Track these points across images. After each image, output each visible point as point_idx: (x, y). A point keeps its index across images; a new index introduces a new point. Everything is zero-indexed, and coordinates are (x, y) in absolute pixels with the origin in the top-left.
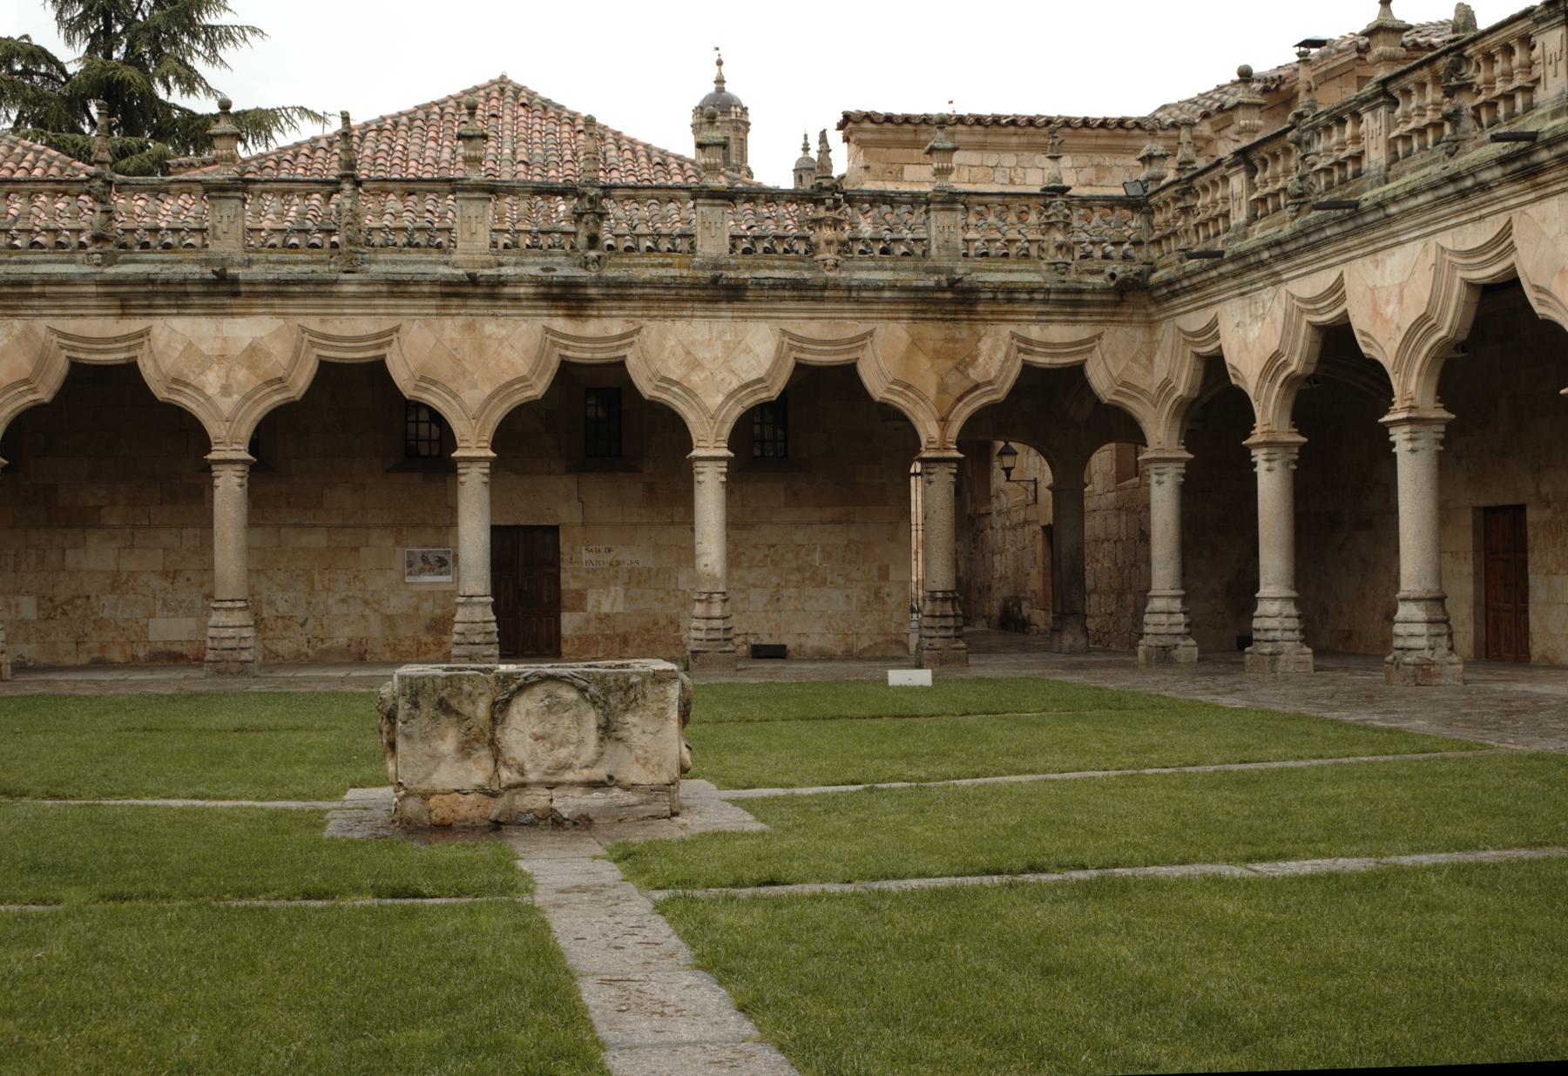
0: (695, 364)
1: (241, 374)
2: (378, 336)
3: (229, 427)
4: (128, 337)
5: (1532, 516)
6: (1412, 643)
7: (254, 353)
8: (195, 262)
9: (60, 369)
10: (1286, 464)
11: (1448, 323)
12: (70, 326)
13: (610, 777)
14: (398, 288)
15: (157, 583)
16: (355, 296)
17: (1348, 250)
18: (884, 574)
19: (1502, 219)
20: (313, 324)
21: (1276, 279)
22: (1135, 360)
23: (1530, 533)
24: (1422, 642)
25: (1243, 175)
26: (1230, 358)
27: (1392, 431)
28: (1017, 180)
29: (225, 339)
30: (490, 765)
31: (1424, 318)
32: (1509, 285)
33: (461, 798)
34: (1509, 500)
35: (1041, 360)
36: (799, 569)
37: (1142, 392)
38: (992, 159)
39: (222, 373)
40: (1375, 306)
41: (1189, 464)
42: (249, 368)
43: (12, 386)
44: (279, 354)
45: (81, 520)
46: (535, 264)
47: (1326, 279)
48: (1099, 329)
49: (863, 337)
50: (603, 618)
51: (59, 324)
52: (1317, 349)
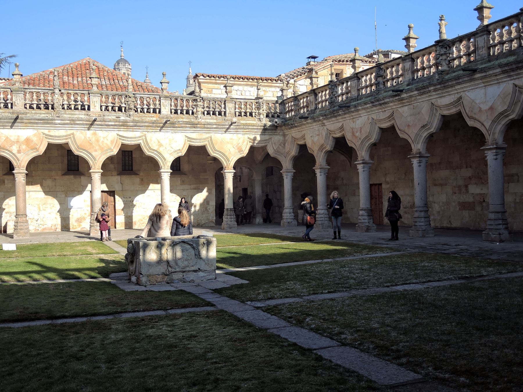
0: (161, 145)
1: (24, 147)
2: (66, 136)
3: (21, 162)
5: (384, 186)
6: (363, 221)
7: (28, 141)
8: (8, 113)
10: (325, 174)
11: (374, 138)
13: (199, 269)
17: (345, 118)
19: (391, 111)
20: (46, 132)
22: (280, 145)
23: (383, 191)
24: (366, 221)
25: (313, 96)
26: (309, 145)
27: (358, 166)
28: (243, 94)
29: (18, 136)
30: (166, 267)
32: (392, 129)
33: (158, 276)
34: (377, 182)
39: (18, 146)
40: (353, 133)
41: (294, 173)
42: (26, 145)
46: (114, 116)
48: (271, 136)
52: (334, 143)
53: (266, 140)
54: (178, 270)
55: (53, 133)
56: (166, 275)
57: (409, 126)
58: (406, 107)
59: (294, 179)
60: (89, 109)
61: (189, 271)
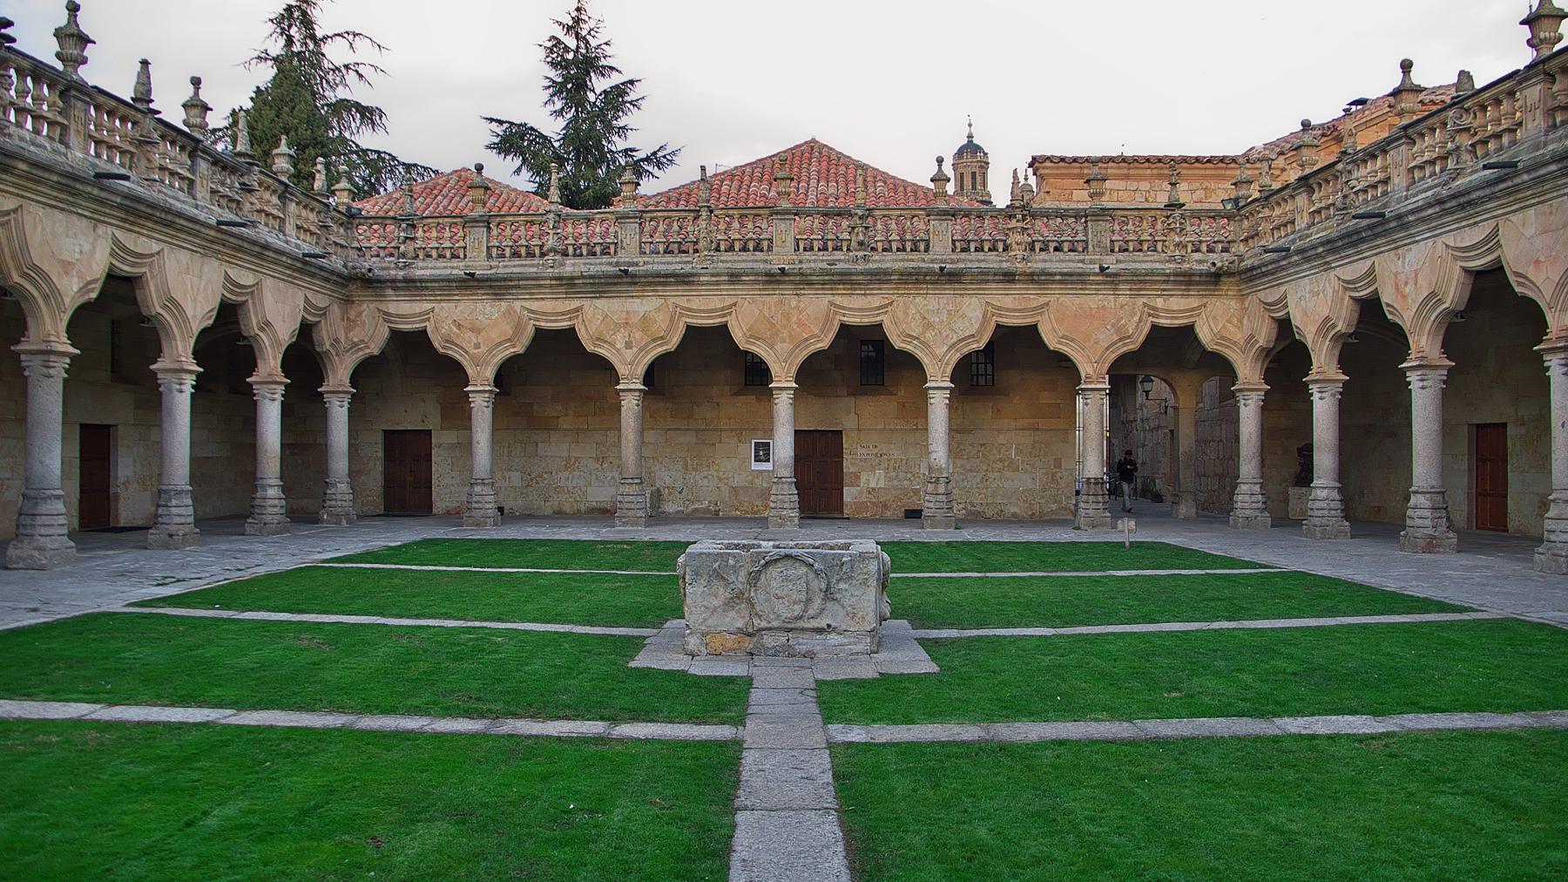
0: (928, 326)
1: (638, 335)
2: (723, 309)
3: (630, 367)
4: (569, 312)
8: (610, 264)
9: (530, 332)
10: (1333, 395)
12: (534, 305)
14: (735, 277)
15: (593, 465)
16: (708, 283)
17: (1378, 246)
18: (1058, 465)
19: (1492, 223)
20: (682, 302)
21: (1327, 267)
22: (1229, 321)
24: (1428, 523)
25: (1304, 195)
26: (1296, 321)
31: (1432, 294)
32: (1497, 270)
35: (1164, 322)
36: (1001, 460)
37: (1234, 343)
38: (1133, 185)
41: (1267, 393)
43: (501, 343)
44: (661, 322)
45: (546, 426)
47: (1362, 267)
49: (1042, 306)
50: (871, 491)
51: (527, 304)
52: (1356, 315)
53: (1192, 310)
54: (775, 624)
55: (696, 303)
56: (750, 635)
57: (1537, 262)
58: (1531, 211)
59: (1266, 408)
60: (770, 249)
61: (803, 630)
